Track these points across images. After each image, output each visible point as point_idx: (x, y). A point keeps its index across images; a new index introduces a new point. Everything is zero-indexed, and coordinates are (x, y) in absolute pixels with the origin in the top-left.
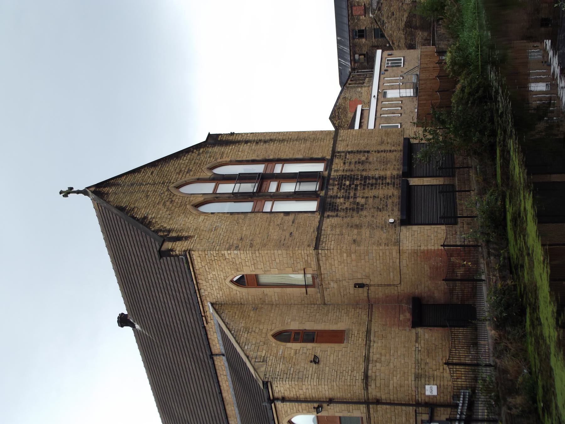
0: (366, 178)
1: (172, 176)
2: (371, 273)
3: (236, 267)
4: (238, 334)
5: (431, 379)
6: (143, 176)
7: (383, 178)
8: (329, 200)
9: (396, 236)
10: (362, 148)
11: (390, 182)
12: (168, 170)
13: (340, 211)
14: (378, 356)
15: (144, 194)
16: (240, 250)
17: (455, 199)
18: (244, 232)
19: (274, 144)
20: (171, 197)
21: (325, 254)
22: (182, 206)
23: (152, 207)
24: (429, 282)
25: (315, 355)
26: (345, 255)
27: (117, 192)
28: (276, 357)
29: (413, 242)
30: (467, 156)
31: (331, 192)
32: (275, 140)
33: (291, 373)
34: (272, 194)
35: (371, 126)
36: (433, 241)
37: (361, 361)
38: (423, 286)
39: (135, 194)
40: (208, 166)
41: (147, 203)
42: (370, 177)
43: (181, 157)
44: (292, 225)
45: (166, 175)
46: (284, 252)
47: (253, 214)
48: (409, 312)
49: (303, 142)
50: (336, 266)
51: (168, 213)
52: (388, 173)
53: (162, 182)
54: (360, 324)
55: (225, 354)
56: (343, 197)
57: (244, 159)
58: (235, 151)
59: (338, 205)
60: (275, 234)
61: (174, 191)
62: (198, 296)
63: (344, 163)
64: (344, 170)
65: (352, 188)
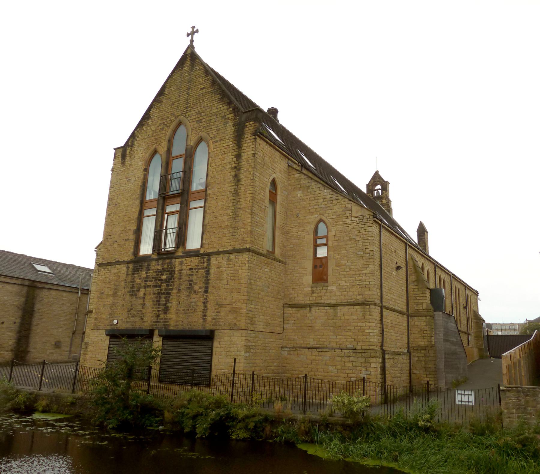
0: (168, 294)
7: (166, 310)
9: (103, 326)
11: (160, 318)
36: (94, 356)
44: (123, 240)
56: (147, 276)
59: (138, 273)
63: (191, 269)
65: (157, 283)
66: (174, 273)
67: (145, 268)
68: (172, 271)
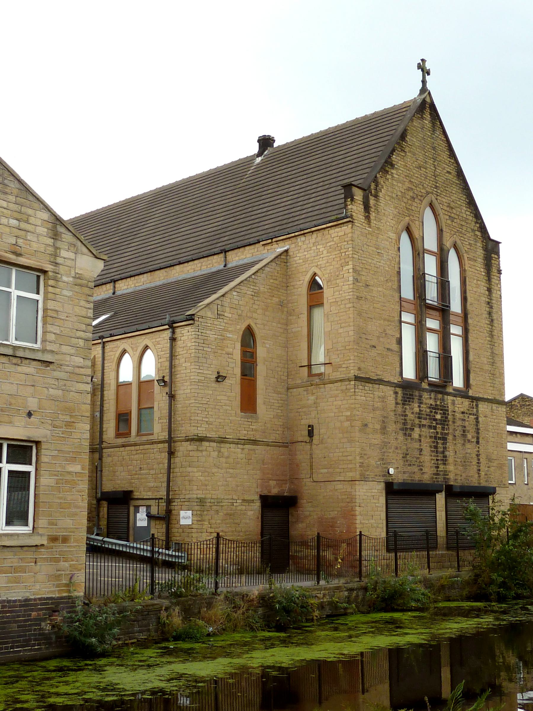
0: (445, 439)
1: (446, 198)
2: (326, 445)
3: (332, 279)
4: (250, 283)
5: (199, 517)
6: (445, 161)
7: (445, 460)
8: (417, 393)
10: (482, 434)
12: (454, 192)
13: (403, 408)
14: (226, 454)
15: (422, 163)
16: (354, 284)
17: (418, 549)
18: (375, 289)
19: (487, 324)
20: (419, 197)
21: (349, 390)
22: (408, 211)
23: (406, 174)
24: (315, 517)
25: (226, 377)
26: (348, 413)
27: (424, 129)
28: (224, 330)
29: (365, 497)
30: (473, 566)
31: (426, 397)
32: (492, 326)
33: (205, 349)
34: (424, 323)
35: (511, 446)
37: (220, 433)
38: (311, 509)
39: (422, 152)
40: (459, 242)
41: (411, 167)
42: (446, 444)
43: (469, 208)
45: (447, 190)
46: (352, 339)
47: (398, 300)
48: (279, 491)
49: (490, 360)
50: (335, 403)
51: (399, 194)
52: (451, 468)
53: (437, 185)
54: (264, 432)
55: (226, 268)
56: (420, 410)
57: (468, 287)
58: (478, 275)
59: (409, 405)
60: (374, 327)
61: (426, 201)
62: (296, 234)
63: (463, 413)
64: (454, 412)
65: (432, 423)
66: (448, 414)
67: (416, 400)
68: (446, 410)
